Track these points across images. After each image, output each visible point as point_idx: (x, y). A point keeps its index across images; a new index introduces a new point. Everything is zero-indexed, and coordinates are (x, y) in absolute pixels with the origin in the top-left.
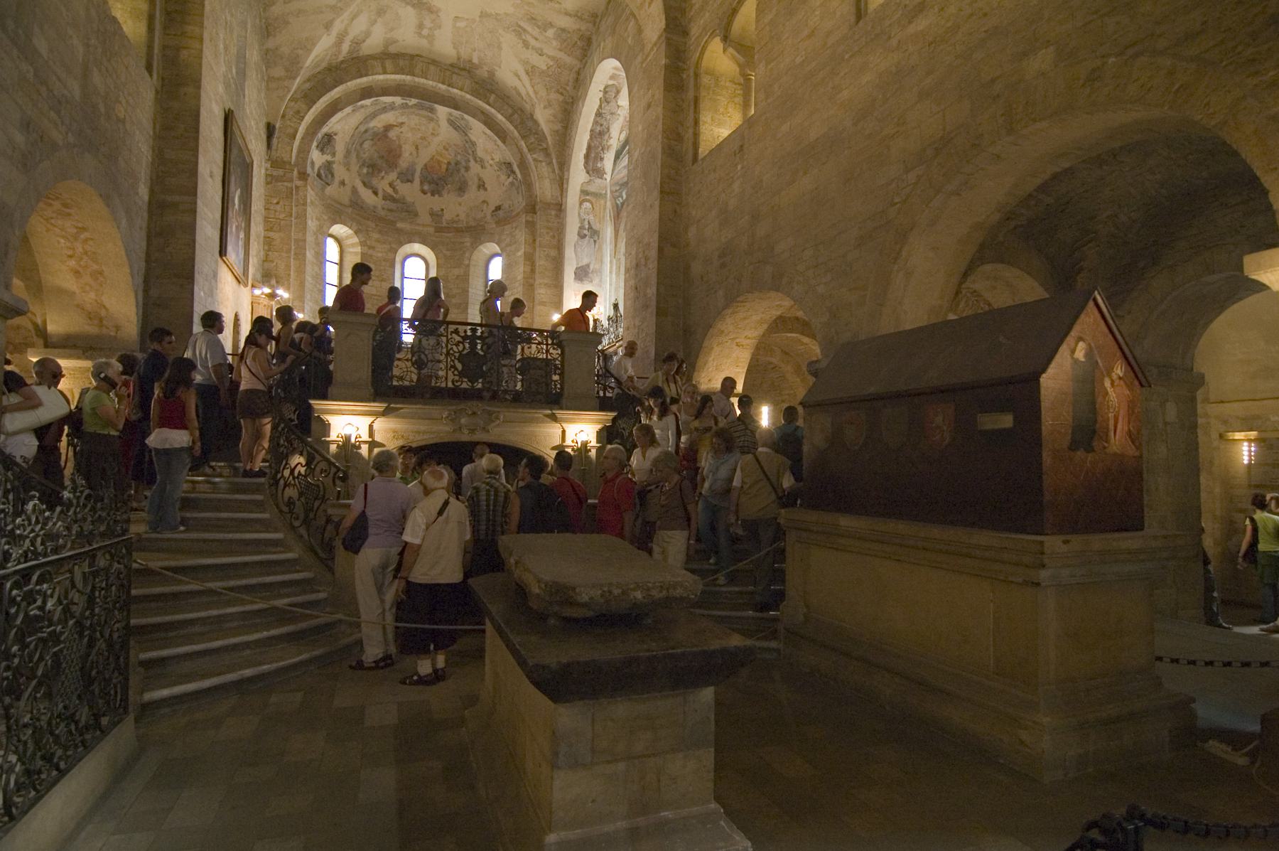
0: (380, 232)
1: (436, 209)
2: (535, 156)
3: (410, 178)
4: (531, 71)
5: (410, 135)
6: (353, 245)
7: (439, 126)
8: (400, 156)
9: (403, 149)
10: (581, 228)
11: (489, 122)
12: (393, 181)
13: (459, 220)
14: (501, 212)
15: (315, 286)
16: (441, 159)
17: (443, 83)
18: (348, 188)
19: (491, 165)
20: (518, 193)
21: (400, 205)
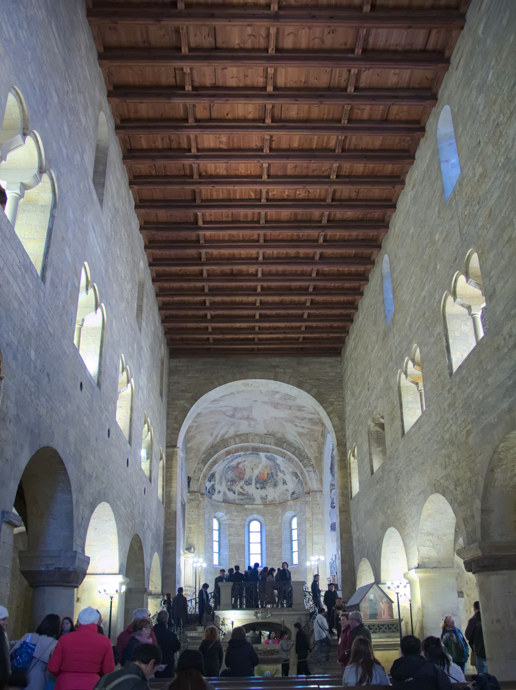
0: (237, 512)
1: (264, 495)
2: (307, 469)
3: (250, 483)
4: (300, 435)
6: (225, 520)
8: (244, 474)
10: (332, 503)
11: (283, 456)
14: (295, 496)
17: (262, 443)
18: (222, 494)
21: (246, 496)
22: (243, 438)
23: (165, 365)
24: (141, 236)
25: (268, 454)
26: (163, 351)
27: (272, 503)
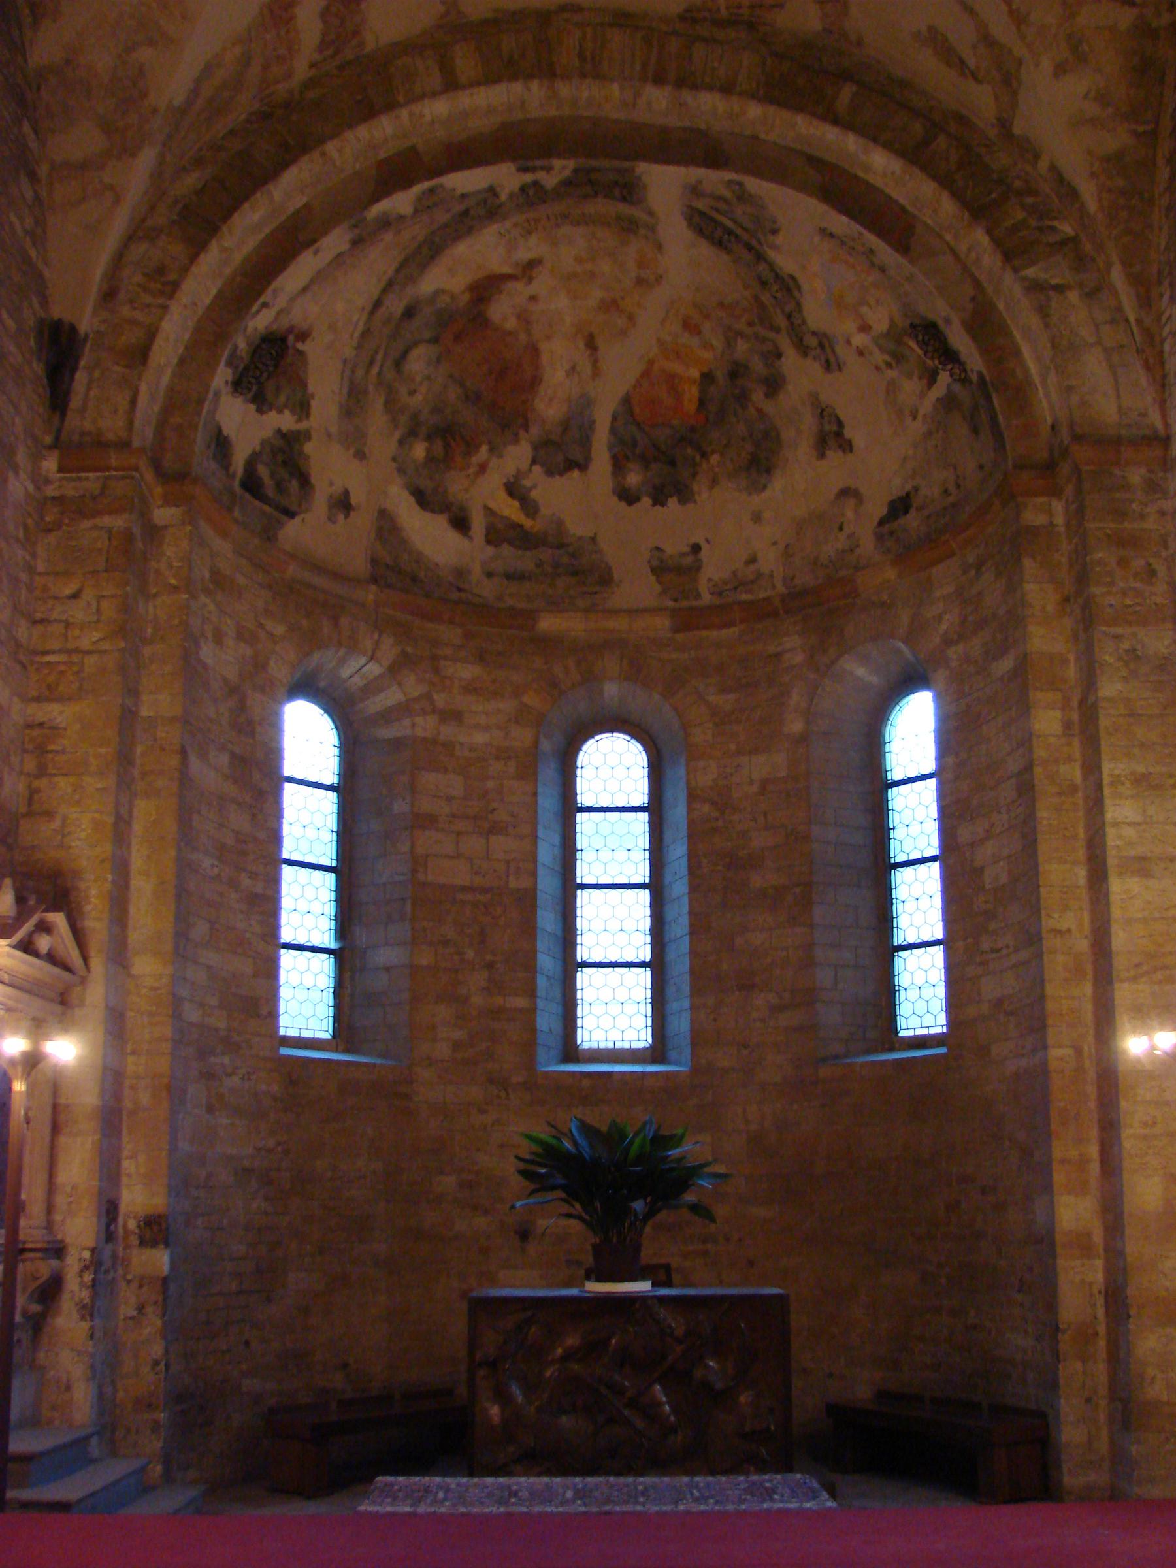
0: (481, 658)
2: (1031, 272)
5: (562, 302)
6: (387, 716)
7: (660, 247)
8: (535, 381)
9: (545, 358)
12: (519, 475)
13: (759, 575)
14: (912, 521)
15: (233, 884)
16: (676, 367)
17: (659, 80)
18: (363, 522)
19: (861, 353)
20: (975, 430)
21: (545, 554)
25: (714, 179)
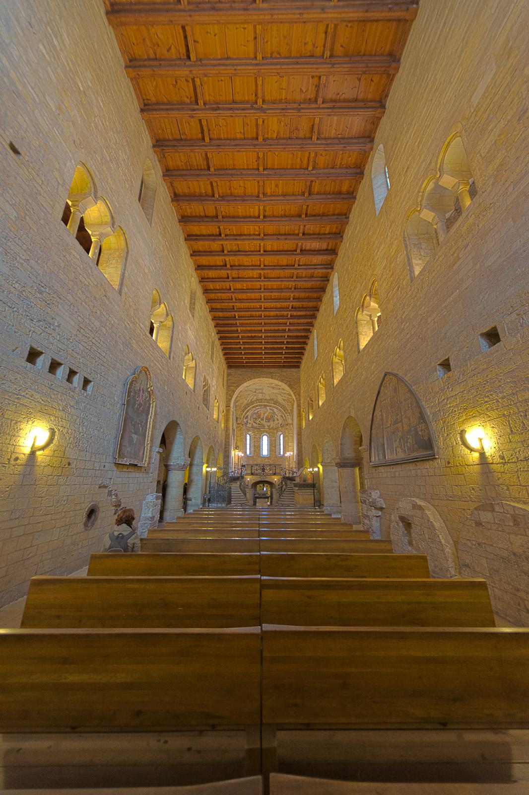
11: (277, 408)
18: (251, 424)
22: (260, 401)
23: (225, 373)
24: (213, 323)
26: (225, 366)
27: (273, 428)
